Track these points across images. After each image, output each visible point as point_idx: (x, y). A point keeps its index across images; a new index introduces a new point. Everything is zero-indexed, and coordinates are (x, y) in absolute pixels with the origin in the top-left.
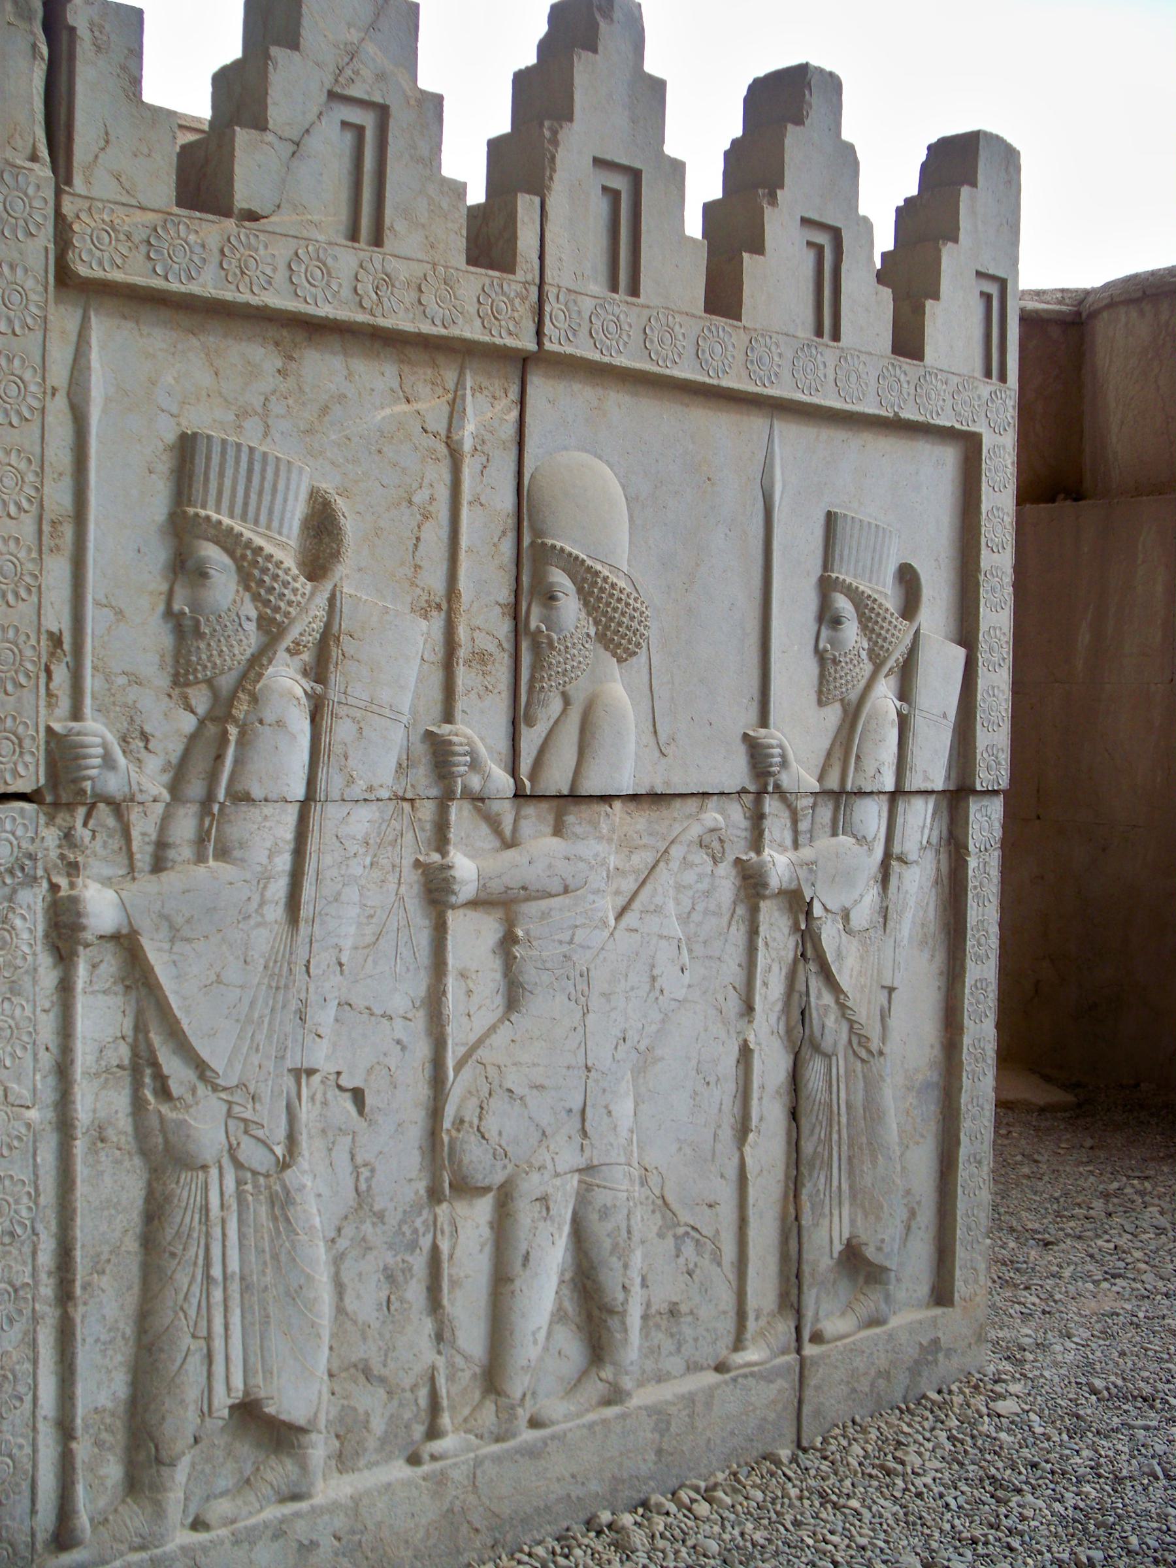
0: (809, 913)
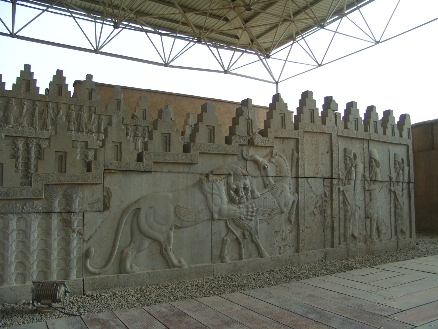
0: (396, 194)
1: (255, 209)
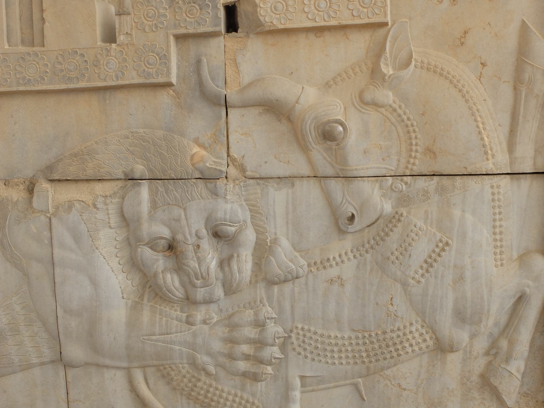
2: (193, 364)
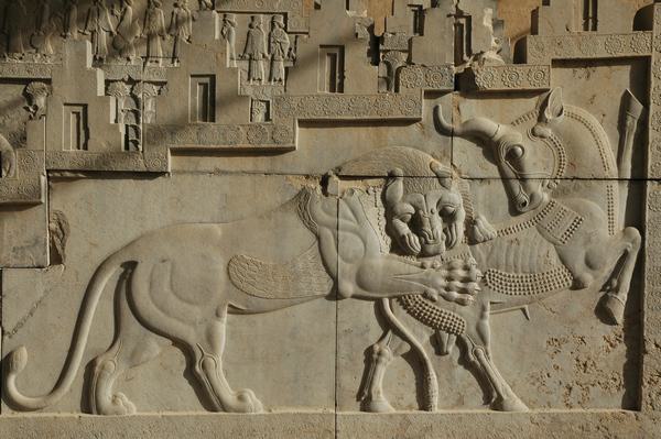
1: (477, 272)
2: (425, 295)
